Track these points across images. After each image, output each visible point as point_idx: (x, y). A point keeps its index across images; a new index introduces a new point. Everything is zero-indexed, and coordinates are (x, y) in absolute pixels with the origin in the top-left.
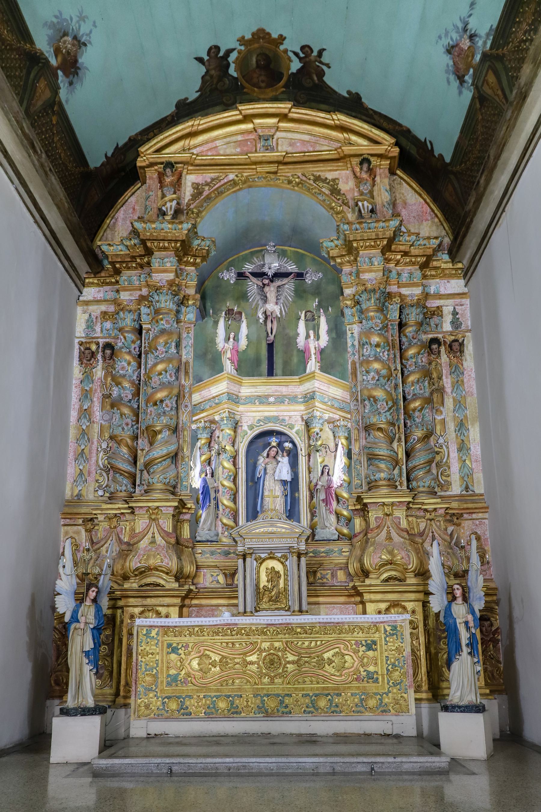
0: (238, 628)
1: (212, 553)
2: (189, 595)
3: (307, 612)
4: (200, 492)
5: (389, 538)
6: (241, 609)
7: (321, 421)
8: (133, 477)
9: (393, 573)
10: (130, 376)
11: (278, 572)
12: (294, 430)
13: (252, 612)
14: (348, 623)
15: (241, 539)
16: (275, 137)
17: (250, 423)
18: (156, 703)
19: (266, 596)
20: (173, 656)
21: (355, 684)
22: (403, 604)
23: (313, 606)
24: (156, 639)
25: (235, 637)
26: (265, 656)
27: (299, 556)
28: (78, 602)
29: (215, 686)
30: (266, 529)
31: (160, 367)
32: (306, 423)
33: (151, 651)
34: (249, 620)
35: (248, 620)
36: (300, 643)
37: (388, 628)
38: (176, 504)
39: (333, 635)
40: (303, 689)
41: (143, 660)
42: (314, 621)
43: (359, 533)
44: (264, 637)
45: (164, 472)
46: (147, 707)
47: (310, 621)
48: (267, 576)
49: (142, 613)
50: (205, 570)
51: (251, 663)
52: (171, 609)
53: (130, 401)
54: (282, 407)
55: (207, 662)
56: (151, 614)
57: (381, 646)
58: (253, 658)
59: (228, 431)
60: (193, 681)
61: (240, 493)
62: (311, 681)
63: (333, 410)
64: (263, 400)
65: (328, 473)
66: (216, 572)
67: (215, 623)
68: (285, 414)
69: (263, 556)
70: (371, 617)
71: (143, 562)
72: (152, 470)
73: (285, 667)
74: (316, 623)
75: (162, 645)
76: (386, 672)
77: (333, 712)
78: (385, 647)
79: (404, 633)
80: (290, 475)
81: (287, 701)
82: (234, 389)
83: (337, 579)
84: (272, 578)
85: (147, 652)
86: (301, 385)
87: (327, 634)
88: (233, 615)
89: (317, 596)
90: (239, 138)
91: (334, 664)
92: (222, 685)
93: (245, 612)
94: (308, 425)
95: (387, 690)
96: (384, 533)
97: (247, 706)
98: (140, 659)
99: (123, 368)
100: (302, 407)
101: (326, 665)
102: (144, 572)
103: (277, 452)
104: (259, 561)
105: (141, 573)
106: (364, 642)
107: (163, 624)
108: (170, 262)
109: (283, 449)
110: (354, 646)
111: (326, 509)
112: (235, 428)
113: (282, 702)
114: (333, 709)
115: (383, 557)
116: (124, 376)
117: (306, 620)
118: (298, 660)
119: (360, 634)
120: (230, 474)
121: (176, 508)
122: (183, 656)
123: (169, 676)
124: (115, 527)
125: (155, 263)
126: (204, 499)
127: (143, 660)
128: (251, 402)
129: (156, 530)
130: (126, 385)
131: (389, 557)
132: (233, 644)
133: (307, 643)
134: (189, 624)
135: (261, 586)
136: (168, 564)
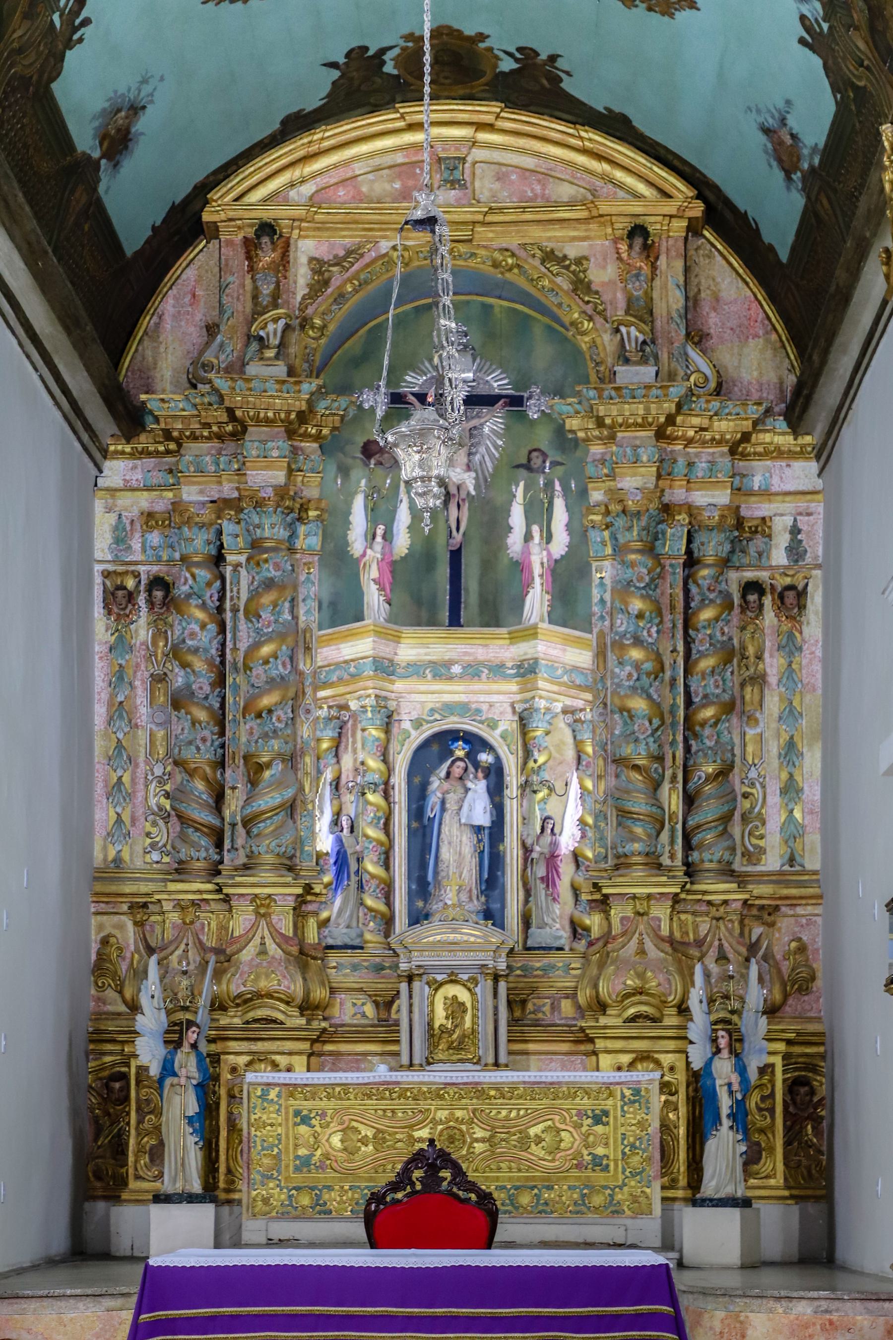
1: (355, 967)
3: (507, 1066)
4: (332, 861)
5: (642, 951)
6: (405, 1060)
7: (548, 717)
9: (644, 1008)
11: (463, 1004)
12: (498, 732)
13: (421, 1065)
14: (567, 1083)
15: (404, 950)
17: (414, 715)
18: (279, 1196)
20: (303, 1129)
21: (575, 1173)
22: (656, 1056)
23: (518, 1057)
24: (276, 1103)
25: (396, 1102)
26: (442, 1131)
27: (496, 978)
28: (171, 1047)
29: (366, 1172)
30: (443, 937)
32: (521, 719)
33: (269, 1121)
36: (494, 1112)
37: (628, 1093)
39: (544, 1101)
40: (497, 1179)
41: (258, 1133)
42: (515, 1079)
43: (598, 939)
44: (440, 1103)
46: (266, 1201)
47: (510, 1080)
48: (446, 1009)
54: (477, 686)
55: (355, 1138)
56: (263, 1066)
57: (615, 1118)
59: (374, 732)
60: (334, 1165)
62: (510, 1168)
63: (573, 692)
65: (552, 830)
66: (361, 998)
67: (366, 1081)
68: (482, 698)
69: (439, 978)
70: (607, 1075)
71: (249, 984)
72: (255, 831)
73: (471, 1146)
74: (519, 1083)
75: (287, 1113)
76: (620, 1157)
77: (540, 1212)
78: (621, 1120)
79: (651, 1100)
80: (488, 815)
82: (385, 649)
83: (560, 1012)
85: (264, 1122)
86: (511, 644)
87: (534, 1099)
89: (526, 1041)
91: (543, 1143)
92: (376, 1172)
93: (411, 1065)
94: (523, 722)
95: (620, 1183)
96: (633, 944)
98: (253, 1133)
100: (513, 687)
101: (533, 1145)
102: (251, 1000)
104: (434, 987)
105: (246, 1001)
106: (589, 1113)
107: (287, 1082)
110: (575, 1118)
111: (547, 895)
112: (388, 724)
114: (541, 1208)
115: (629, 982)
118: (492, 1137)
119: (586, 1101)
122: (318, 1129)
124: (192, 923)
127: (258, 1133)
128: (417, 673)
129: (266, 932)
131: (638, 983)
132: (393, 1111)
133: (504, 1113)
134: (327, 1081)
135: (437, 1025)
136: (289, 988)
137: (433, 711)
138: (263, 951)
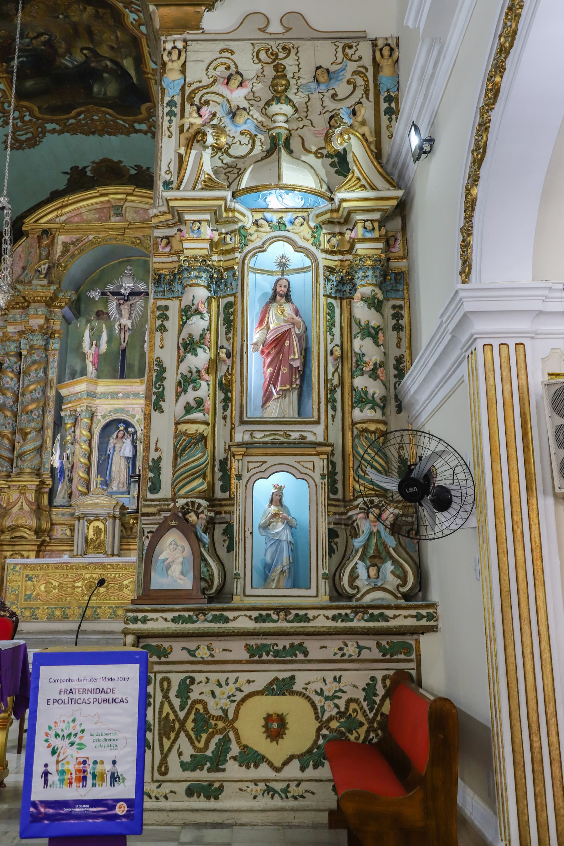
1: (63, 515)
2: (43, 543)
8: (11, 461)
10: (12, 389)
16: (125, 206)
17: (103, 413)
20: (29, 583)
31: (32, 387)
38: (37, 483)
45: (31, 460)
49: (12, 555)
51: (78, 587)
52: (31, 553)
53: (11, 407)
54: (128, 401)
55: (50, 586)
58: (79, 584)
59: (86, 420)
64: (114, 396)
66: (65, 527)
81: (98, 611)
82: (92, 388)
88: (70, 557)
90: (98, 206)
97: (74, 614)
99: (7, 383)
103: (124, 434)
105: (13, 529)
108: (42, 310)
109: (128, 432)
113: (95, 611)
116: (8, 389)
121: (37, 486)
123: (26, 595)
125: (31, 311)
126: (60, 476)
129: (24, 500)
130: (9, 395)
132: (67, 575)
137: (110, 412)
138: (21, 508)
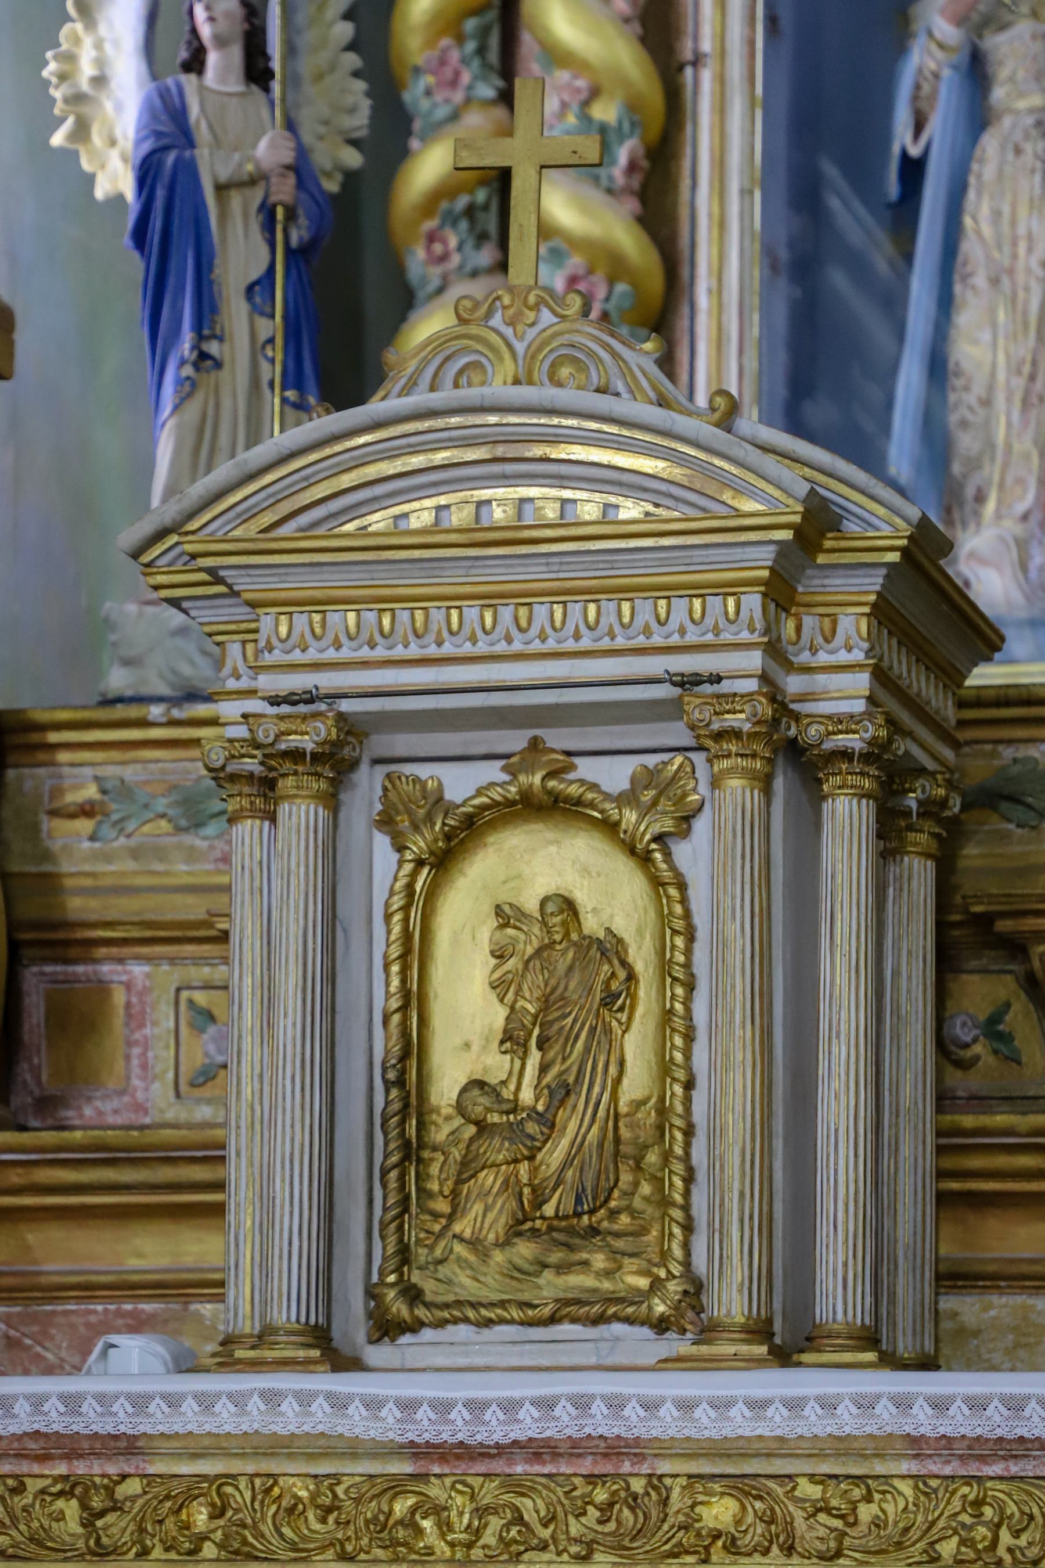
0: (149, 1478)
19: (488, 1179)
34: (238, 1399)
35: (224, 1409)
50: (138, 970)
61: (703, 300)
84: (546, 1003)
117: (777, 1413)
120: (605, 112)
